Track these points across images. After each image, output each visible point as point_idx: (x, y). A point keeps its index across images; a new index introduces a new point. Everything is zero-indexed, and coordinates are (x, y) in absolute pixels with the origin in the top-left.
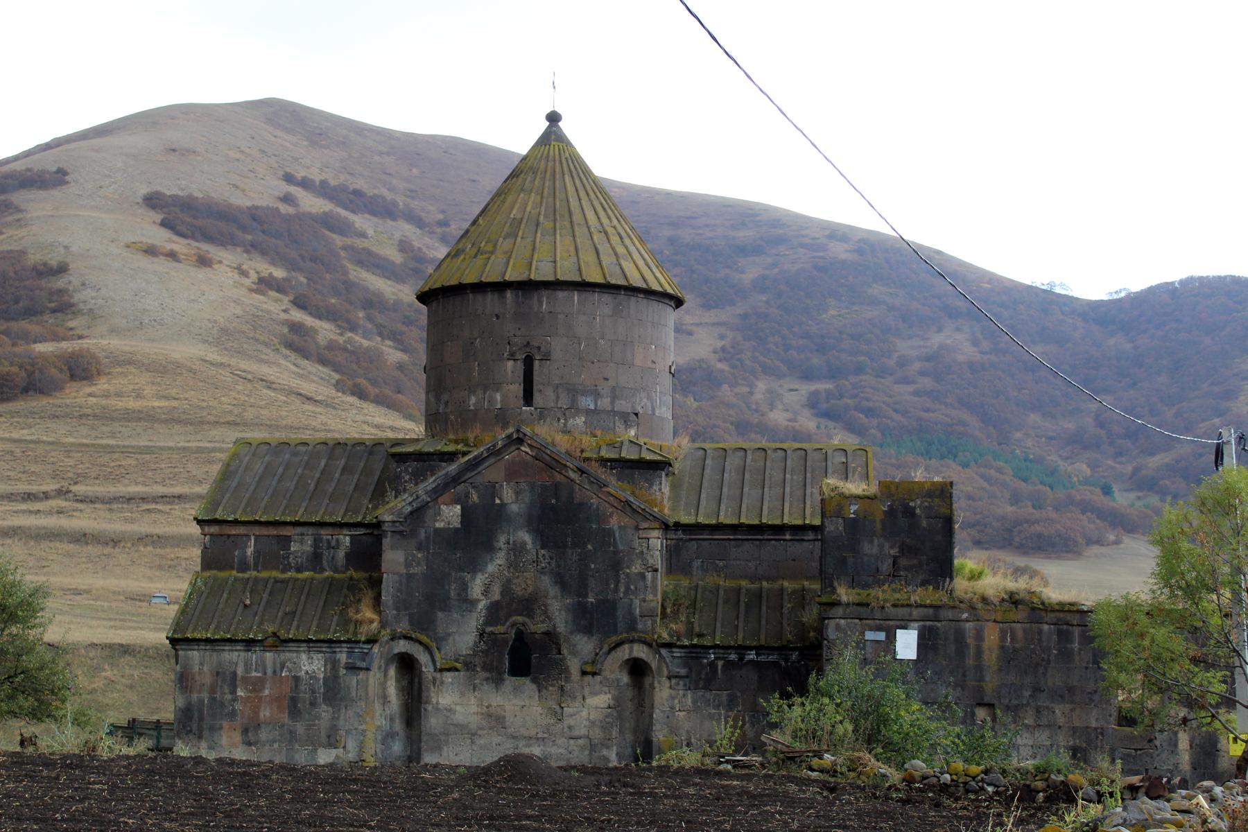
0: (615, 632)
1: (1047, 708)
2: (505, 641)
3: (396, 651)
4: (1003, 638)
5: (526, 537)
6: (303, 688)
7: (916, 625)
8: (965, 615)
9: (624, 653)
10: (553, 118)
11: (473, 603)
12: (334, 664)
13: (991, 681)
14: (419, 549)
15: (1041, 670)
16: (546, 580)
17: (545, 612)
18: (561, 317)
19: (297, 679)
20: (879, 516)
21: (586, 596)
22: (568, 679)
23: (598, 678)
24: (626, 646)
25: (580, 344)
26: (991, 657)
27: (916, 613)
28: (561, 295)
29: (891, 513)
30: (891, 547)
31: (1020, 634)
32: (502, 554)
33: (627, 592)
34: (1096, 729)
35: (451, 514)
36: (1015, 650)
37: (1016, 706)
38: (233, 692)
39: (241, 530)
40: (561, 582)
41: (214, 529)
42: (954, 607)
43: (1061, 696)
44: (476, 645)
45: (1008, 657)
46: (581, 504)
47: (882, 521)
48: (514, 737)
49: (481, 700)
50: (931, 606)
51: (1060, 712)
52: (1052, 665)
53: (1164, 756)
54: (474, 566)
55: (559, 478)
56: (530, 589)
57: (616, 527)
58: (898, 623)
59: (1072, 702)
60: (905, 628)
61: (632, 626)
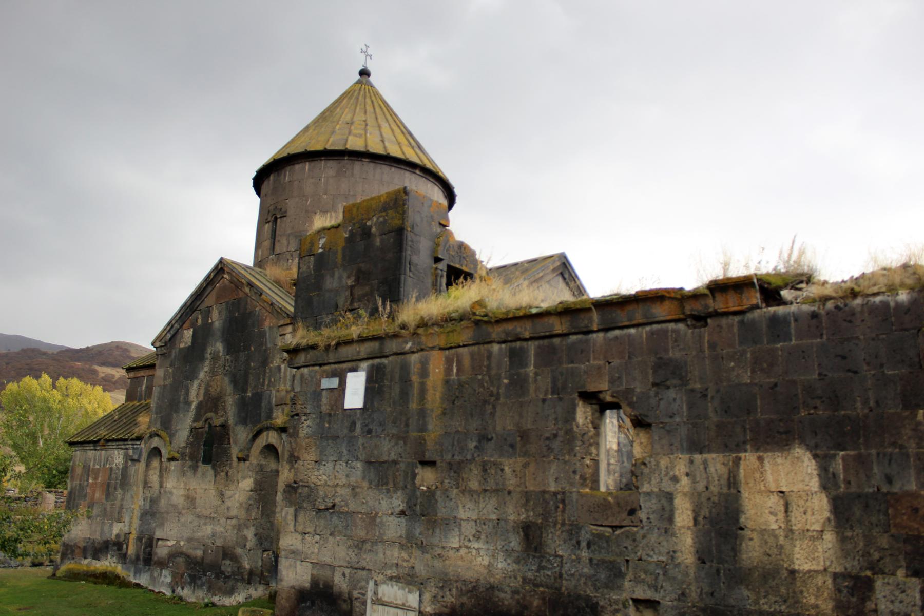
0: (259, 421)
1: (495, 464)
2: (202, 434)
3: (153, 446)
4: (448, 370)
5: (220, 346)
6: (113, 476)
7: (365, 365)
8: (409, 345)
9: (262, 441)
10: (364, 73)
11: (188, 404)
12: (127, 457)
13: (435, 429)
14: (171, 366)
15: (489, 408)
16: (227, 379)
17: (224, 408)
18: (296, 183)
19: (111, 469)
20: (341, 243)
21: (245, 391)
22: (231, 467)
23: (247, 463)
24: (265, 433)
25: (307, 201)
26: (435, 396)
27: (365, 349)
28: (297, 167)
29: (350, 240)
30: (348, 277)
31: (467, 362)
32: (207, 363)
33: (269, 386)
34: (555, 494)
35: (188, 334)
36: (461, 385)
37: (460, 463)
38: (88, 480)
39: (141, 373)
40: (234, 382)
41: (132, 375)
42: (396, 336)
43: (512, 446)
44: (188, 437)
45: (454, 394)
46: (251, 312)
47: (344, 249)
48: (199, 517)
49: (186, 484)
50: (374, 338)
51: (509, 465)
52: (502, 400)
53: (653, 538)
54: (192, 376)
55: (241, 295)
56: (218, 390)
57: (267, 328)
58: (349, 365)
59: (525, 454)
60: (354, 370)
61: (269, 417)
